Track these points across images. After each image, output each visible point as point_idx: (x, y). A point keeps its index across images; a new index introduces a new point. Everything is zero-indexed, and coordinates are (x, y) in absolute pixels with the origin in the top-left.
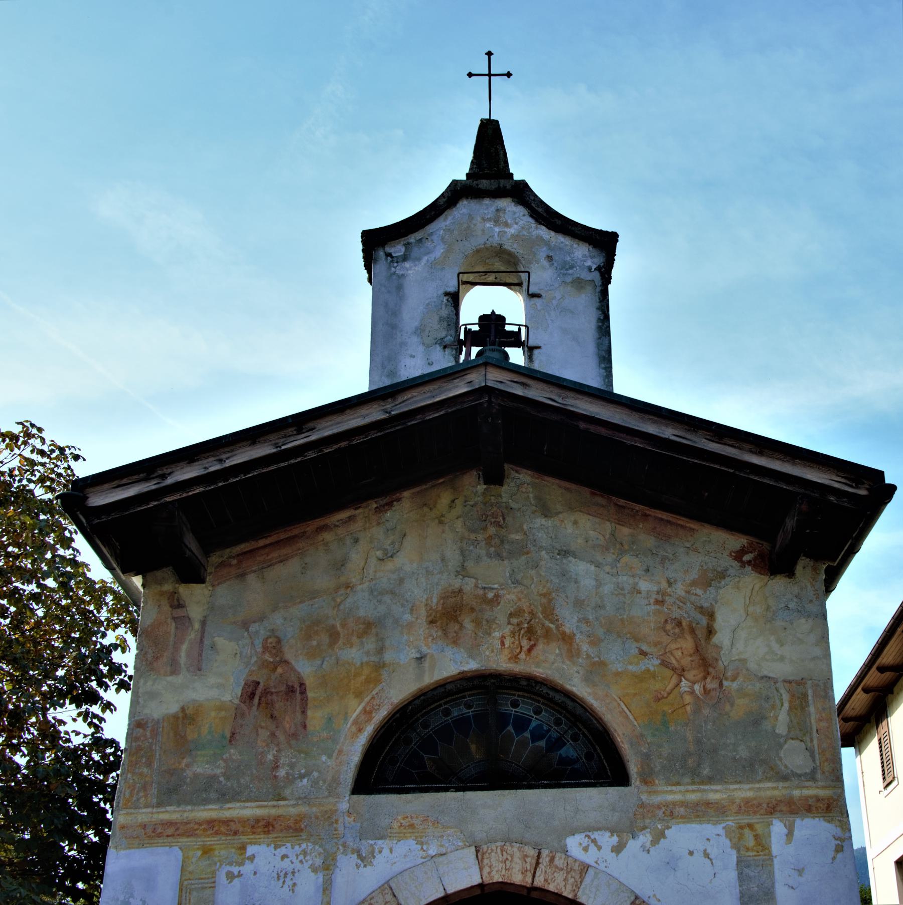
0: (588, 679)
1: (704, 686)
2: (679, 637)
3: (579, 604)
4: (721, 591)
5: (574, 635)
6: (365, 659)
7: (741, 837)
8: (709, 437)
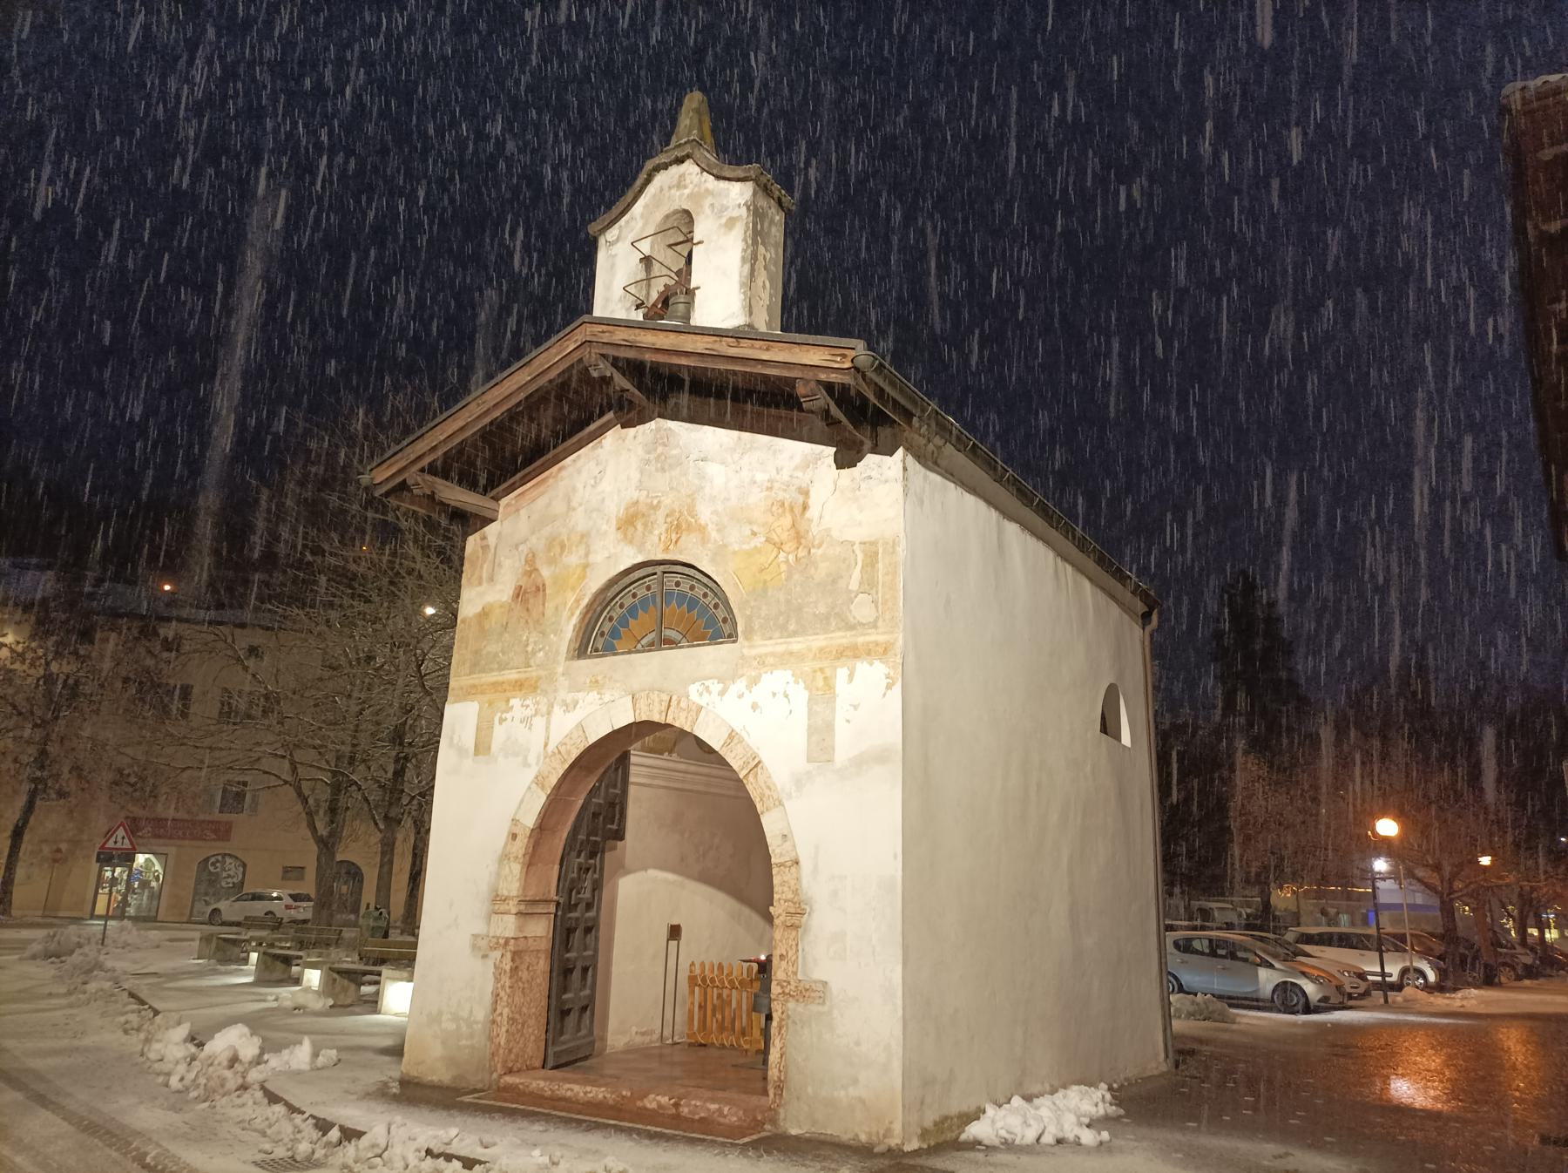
0: (713, 561)
7: (814, 679)
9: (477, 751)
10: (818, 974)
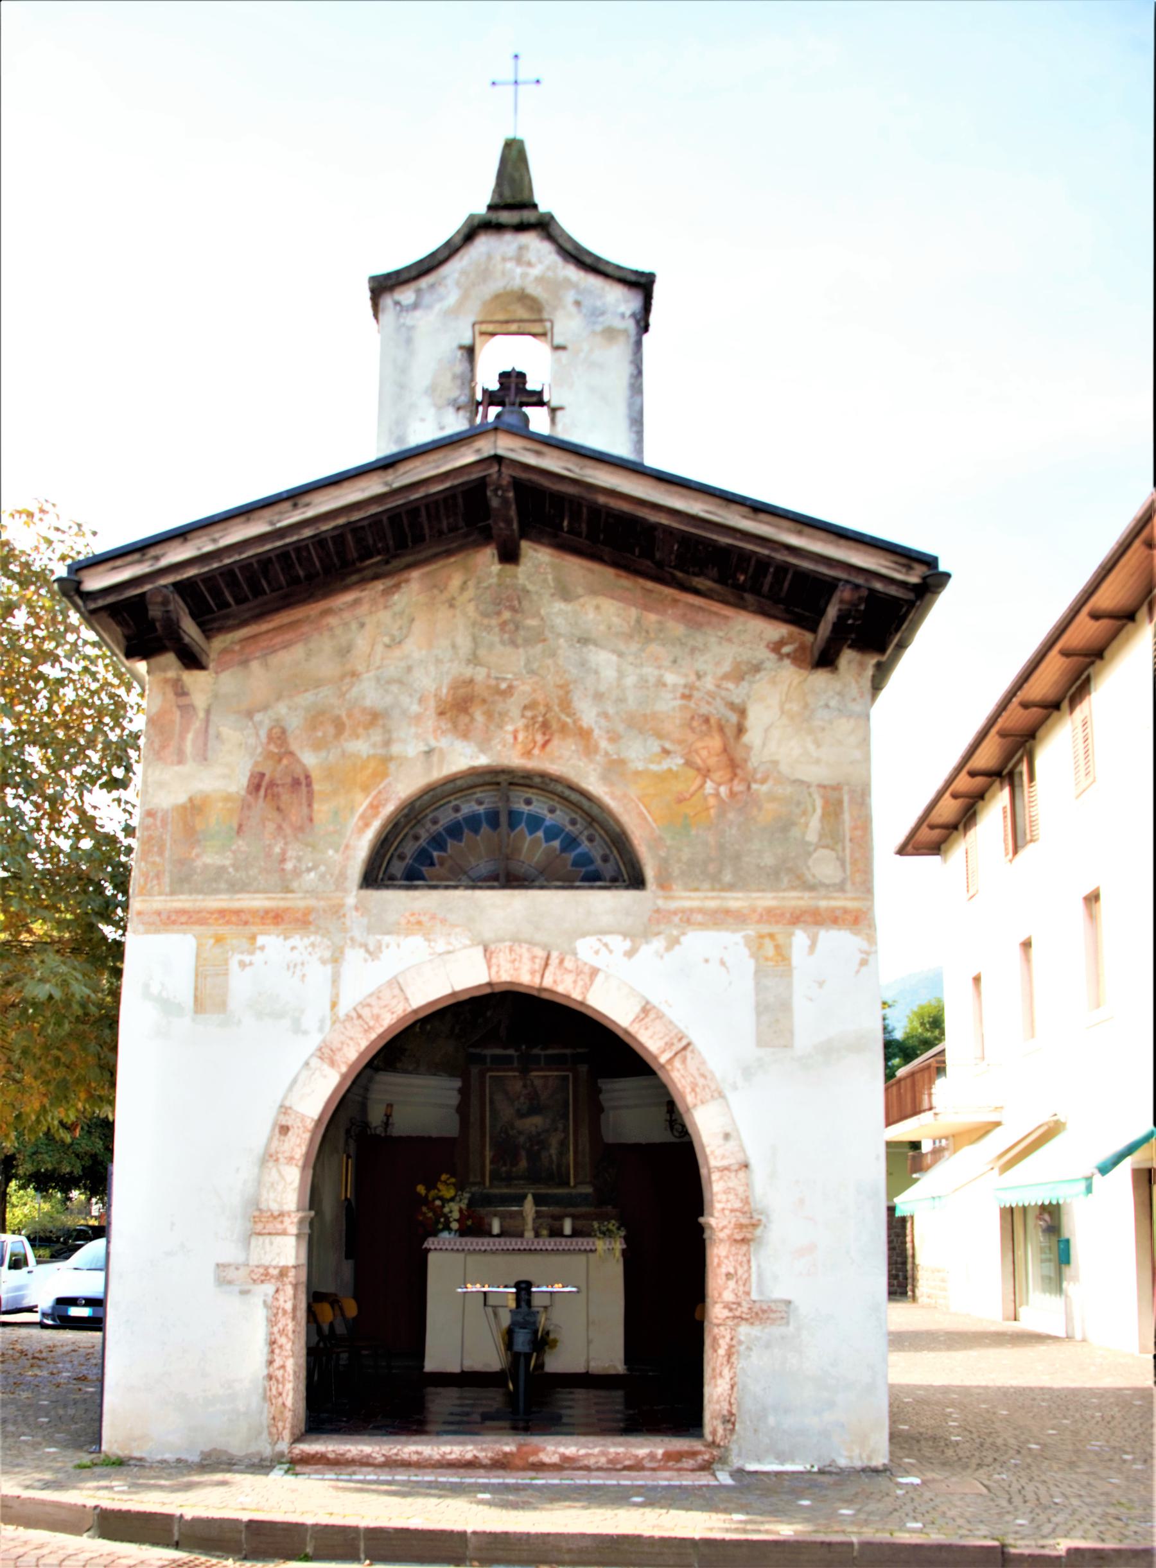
0: (605, 778)
2: (706, 735)
3: (599, 697)
4: (755, 686)
6: (372, 752)
7: (760, 946)
9: (199, 1005)
10: (778, 1292)
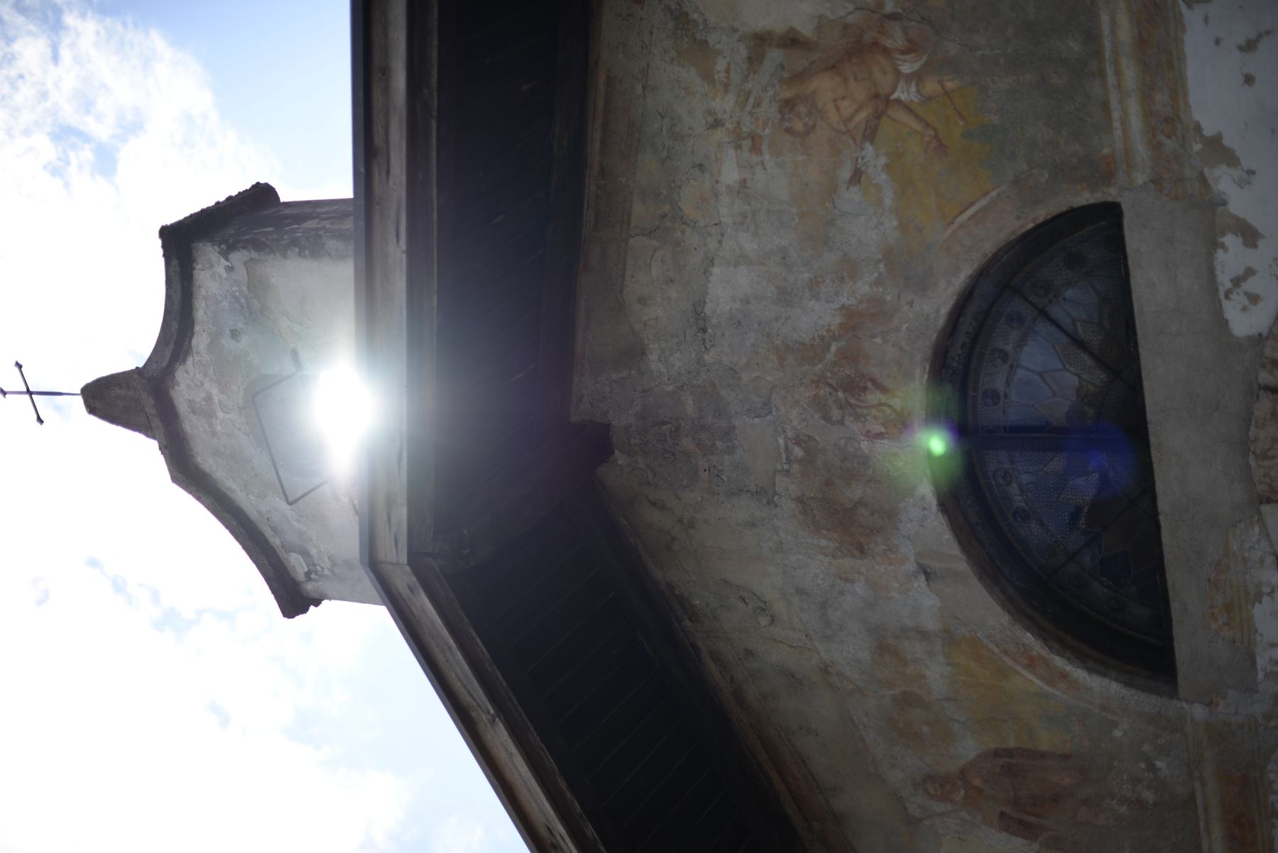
1: (903, 53)
3: (785, 296)
5: (843, 307)
8: (384, 174)
